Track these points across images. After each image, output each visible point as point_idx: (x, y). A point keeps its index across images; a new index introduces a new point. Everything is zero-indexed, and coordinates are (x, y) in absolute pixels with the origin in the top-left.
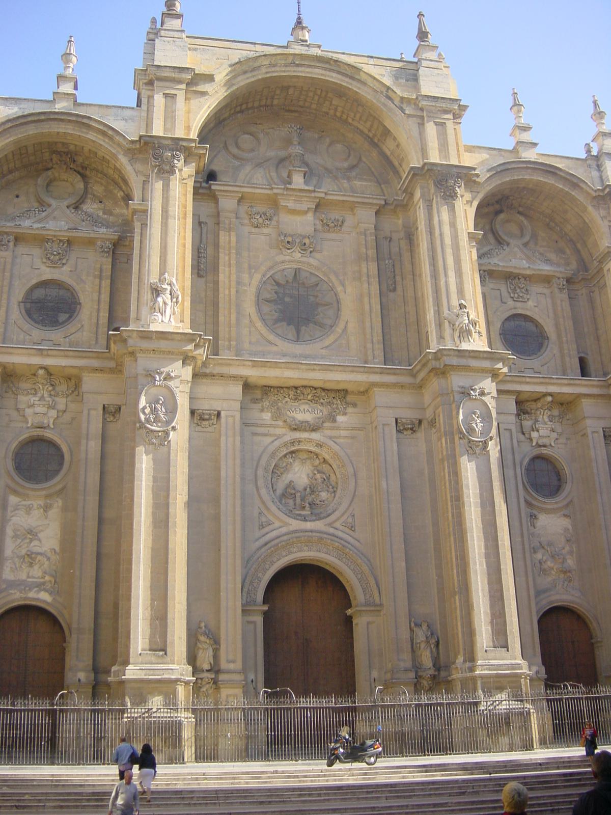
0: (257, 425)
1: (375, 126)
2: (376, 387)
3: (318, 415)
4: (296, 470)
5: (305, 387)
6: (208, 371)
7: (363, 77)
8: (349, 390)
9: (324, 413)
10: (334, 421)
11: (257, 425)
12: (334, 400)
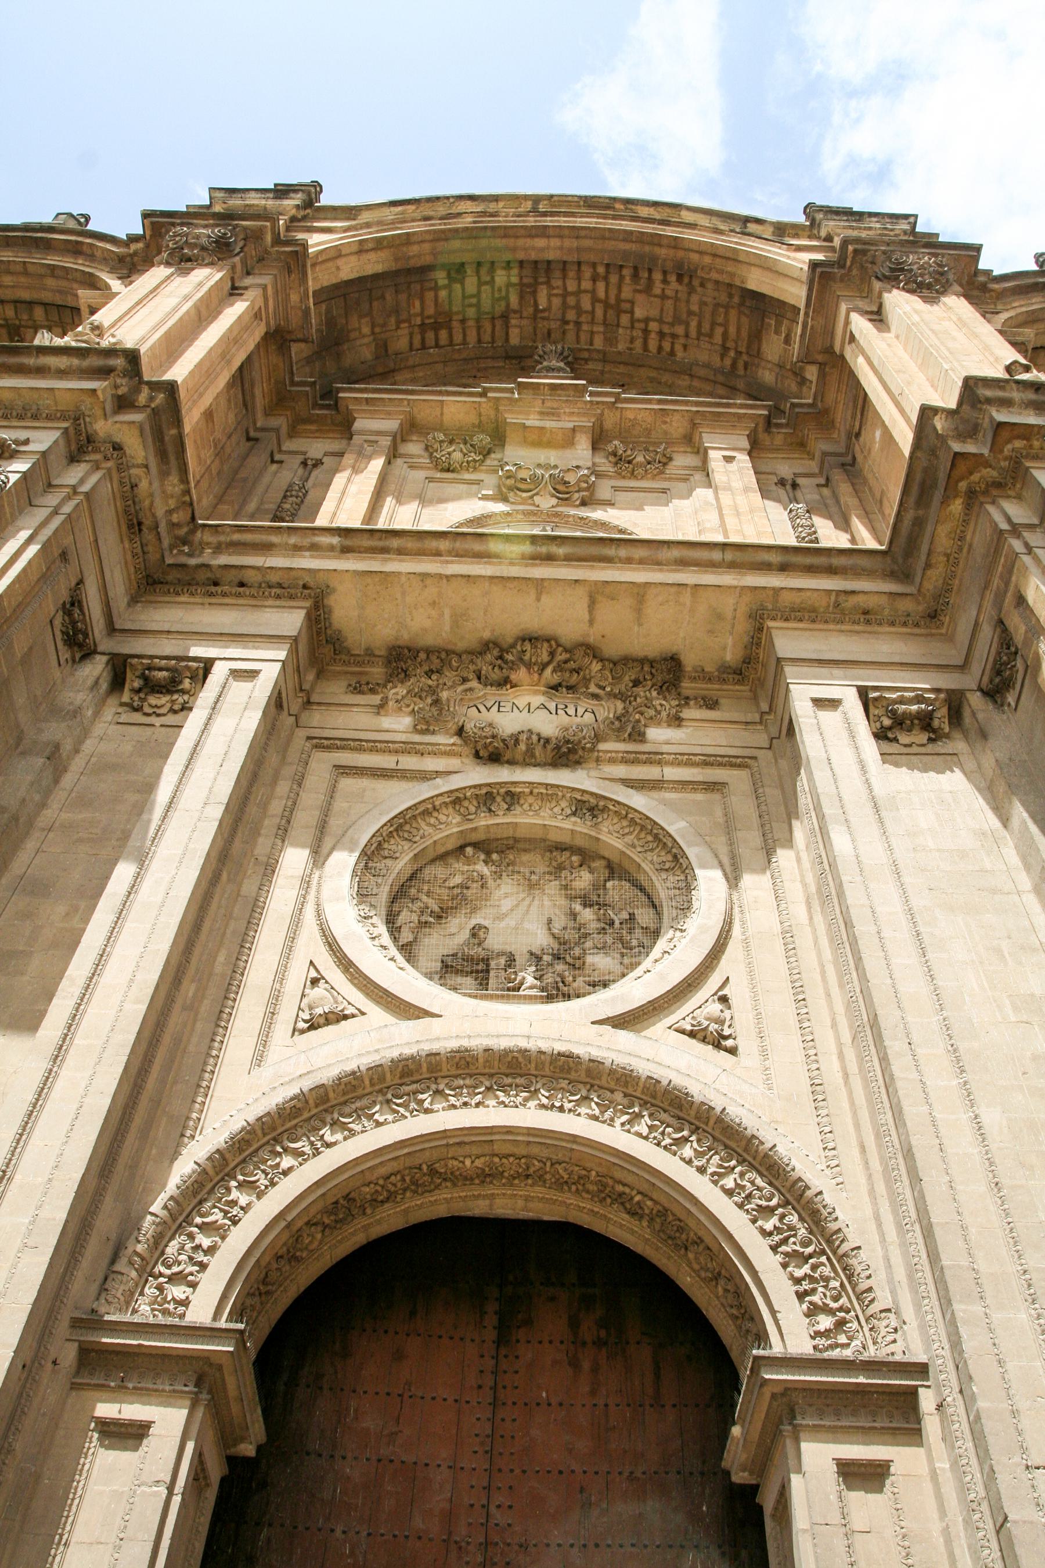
0: (358, 746)
1: (732, 330)
2: (774, 619)
3: (578, 720)
4: (506, 905)
5: (532, 639)
6: (193, 562)
7: (687, 217)
8: (690, 661)
9: (600, 719)
10: (638, 736)
11: (358, 746)
12: (639, 690)
